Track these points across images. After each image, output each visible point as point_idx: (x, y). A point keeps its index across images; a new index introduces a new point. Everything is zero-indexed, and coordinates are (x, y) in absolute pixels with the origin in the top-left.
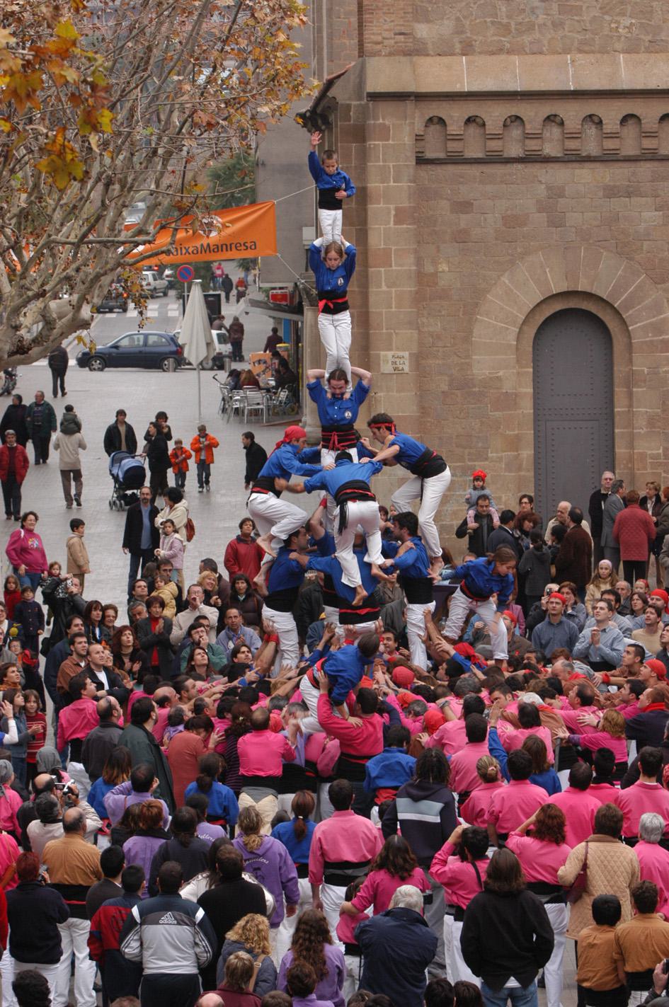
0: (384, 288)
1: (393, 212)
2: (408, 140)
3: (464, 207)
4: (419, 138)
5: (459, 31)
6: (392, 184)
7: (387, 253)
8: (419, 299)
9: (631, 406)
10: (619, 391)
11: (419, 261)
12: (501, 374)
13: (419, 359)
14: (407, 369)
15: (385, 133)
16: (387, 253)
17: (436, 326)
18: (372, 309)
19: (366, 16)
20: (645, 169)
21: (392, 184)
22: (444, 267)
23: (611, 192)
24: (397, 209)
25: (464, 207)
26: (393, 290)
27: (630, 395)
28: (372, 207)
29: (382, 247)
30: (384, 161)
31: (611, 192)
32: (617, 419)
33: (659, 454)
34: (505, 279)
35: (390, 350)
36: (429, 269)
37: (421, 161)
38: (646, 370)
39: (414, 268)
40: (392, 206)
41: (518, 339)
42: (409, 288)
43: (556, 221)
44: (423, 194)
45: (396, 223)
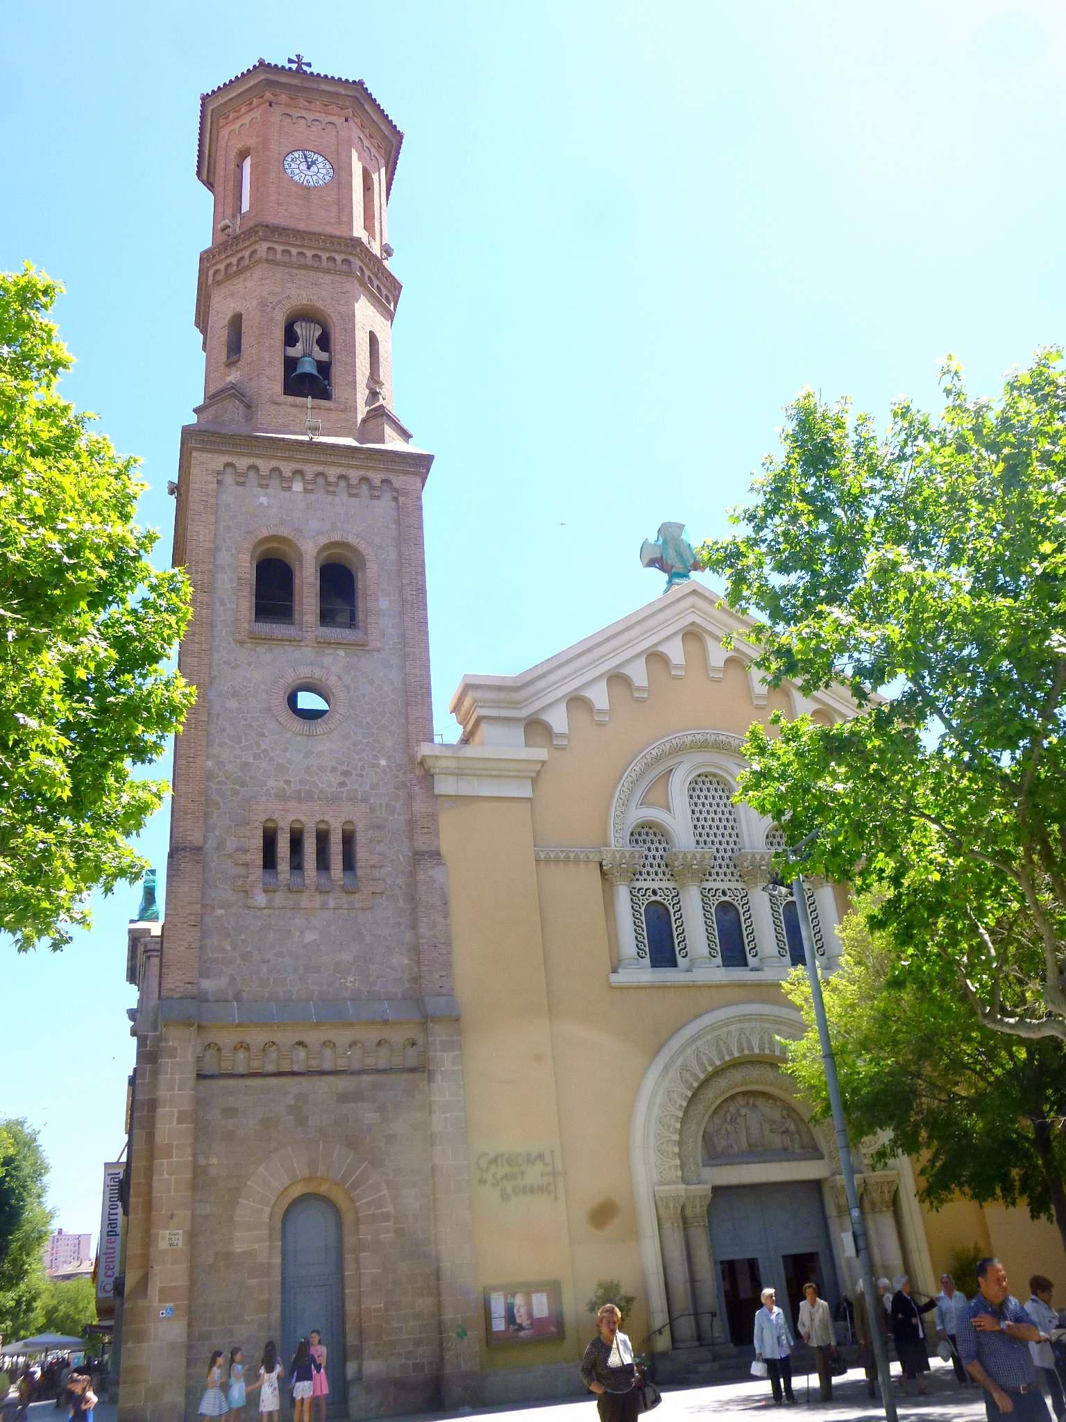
0: (166, 1176)
1: (176, 1115)
2: (190, 1058)
3: (230, 1112)
4: (199, 1059)
5: (232, 980)
6: (177, 1092)
7: (170, 1146)
8: (194, 1185)
9: (358, 1269)
10: (348, 1257)
11: (195, 1155)
12: (257, 1246)
13: (192, 1237)
14: (180, 1244)
15: (173, 1053)
16: (170, 1146)
17: (207, 1209)
18: (155, 1195)
19: (164, 970)
20: (366, 1078)
21: (177, 1092)
22: (214, 1160)
23: (343, 1098)
24: (180, 1112)
25: (230, 1112)
26: (173, 1177)
27: (357, 1260)
28: (160, 1111)
29: (166, 1142)
30: (172, 1074)
31: (343, 1098)
32: (347, 1280)
33: (380, 1308)
34: (261, 1169)
35: (168, 1229)
36: (202, 1161)
37: (201, 1076)
38: (369, 1237)
39: (190, 1159)
40: (176, 1110)
41: (270, 1218)
42: (188, 1175)
43: (302, 1121)
44: (200, 1103)
45: (178, 1123)
